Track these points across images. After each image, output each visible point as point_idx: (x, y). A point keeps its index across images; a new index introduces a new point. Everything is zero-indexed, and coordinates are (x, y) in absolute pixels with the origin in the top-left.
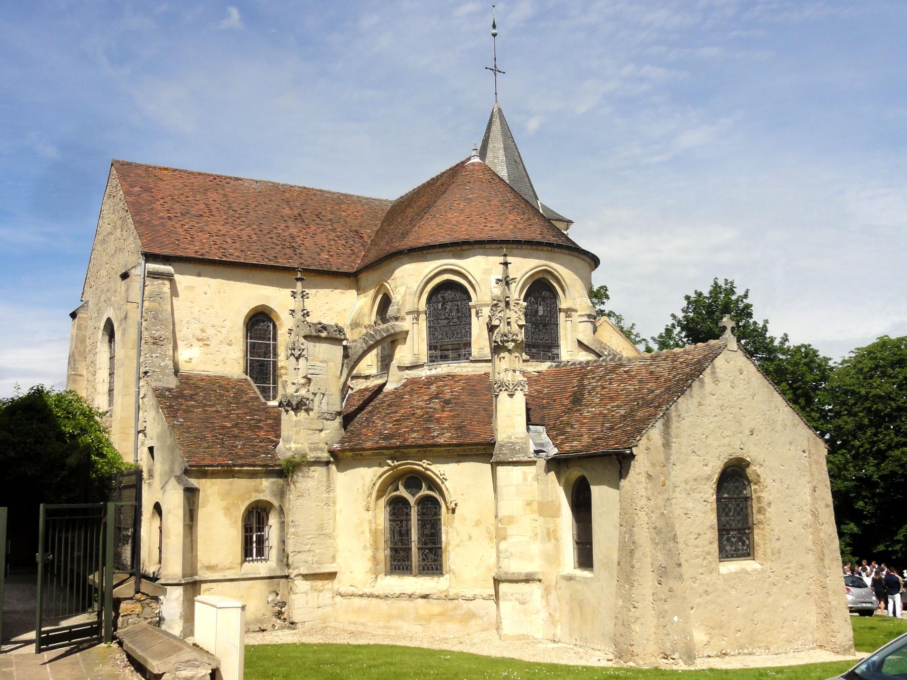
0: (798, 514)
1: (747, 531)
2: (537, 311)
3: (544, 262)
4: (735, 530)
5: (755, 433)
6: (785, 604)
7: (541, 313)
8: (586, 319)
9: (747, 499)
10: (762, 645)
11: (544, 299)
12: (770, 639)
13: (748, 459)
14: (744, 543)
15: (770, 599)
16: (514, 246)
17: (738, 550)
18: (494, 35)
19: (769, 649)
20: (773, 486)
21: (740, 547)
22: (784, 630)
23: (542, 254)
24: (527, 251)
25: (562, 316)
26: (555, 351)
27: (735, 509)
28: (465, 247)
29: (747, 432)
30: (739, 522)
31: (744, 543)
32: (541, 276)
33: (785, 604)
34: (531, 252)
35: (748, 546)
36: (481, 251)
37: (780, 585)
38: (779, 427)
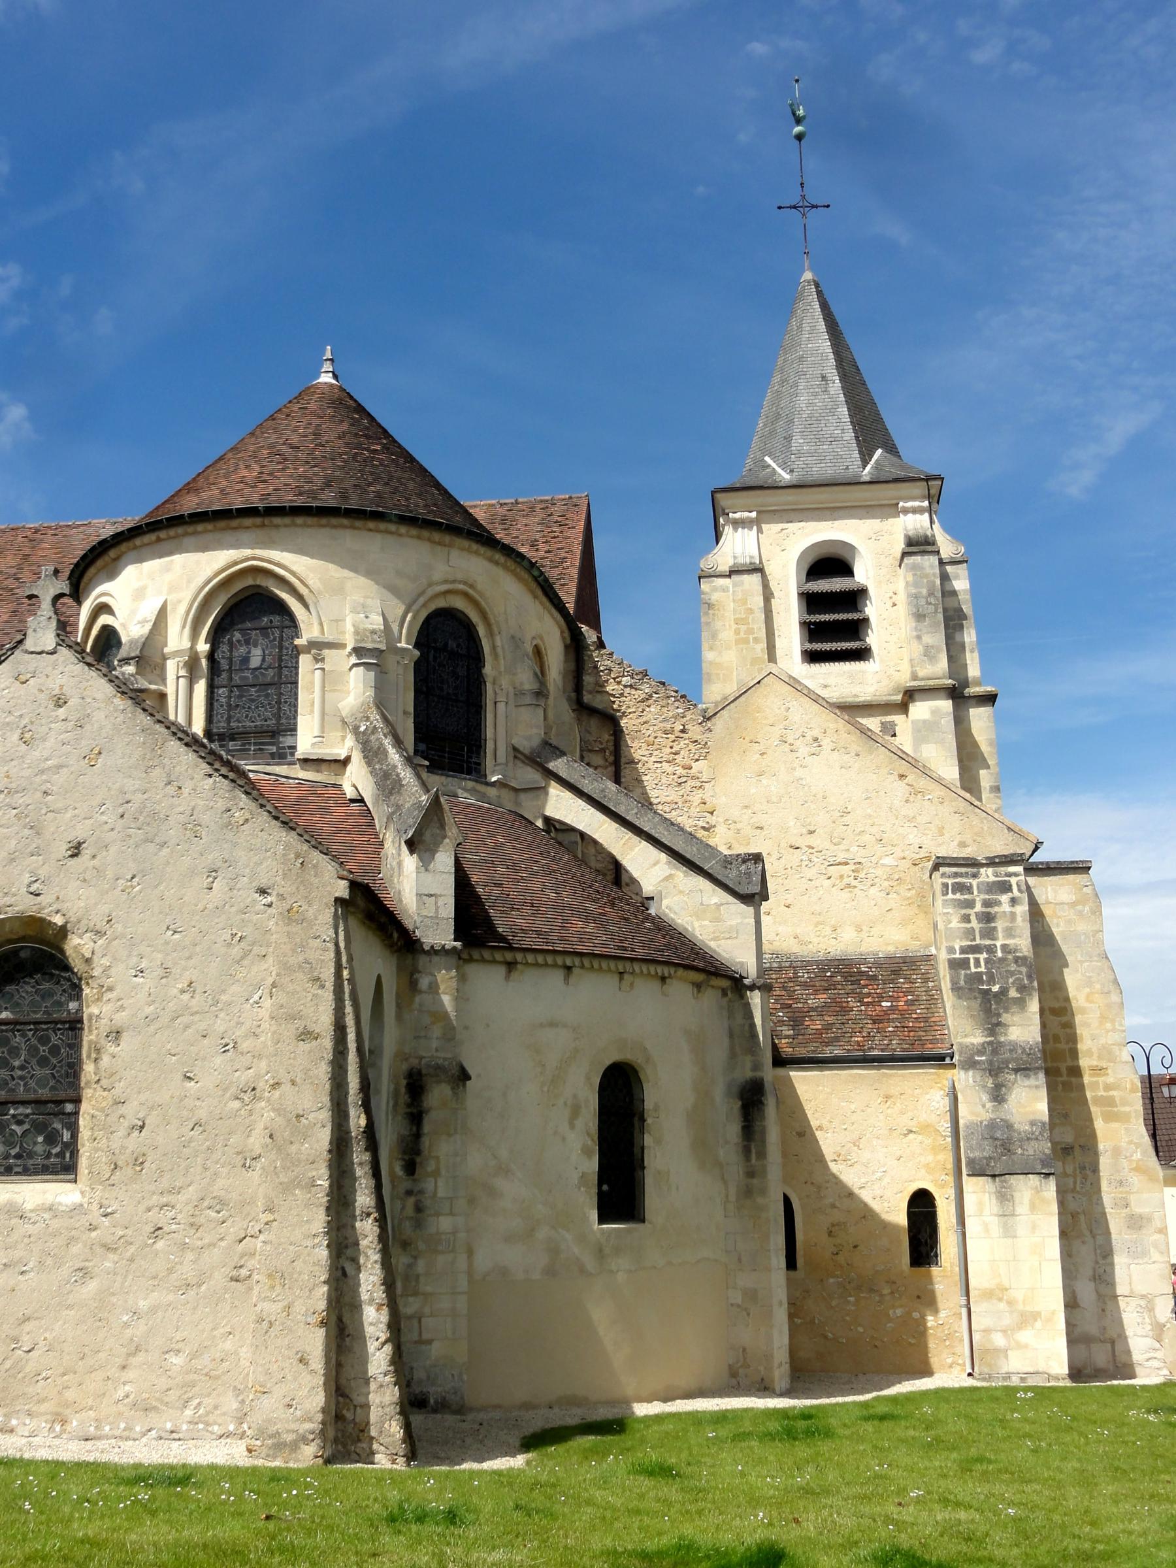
0: (219, 1060)
1: (69, 1107)
2: (246, 660)
3: (248, 552)
4: (23, 1103)
5: (86, 852)
6: (143, 1304)
7: (255, 662)
8: (354, 660)
9: (75, 1025)
10: (43, 1407)
11: (264, 630)
12: (70, 1395)
13: (58, 920)
14: (52, 1139)
15: (92, 1286)
16: (180, 530)
17: (31, 1155)
18: (799, 137)
19: (64, 1422)
20: (135, 987)
21: (39, 1149)
22: (131, 1374)
23: (245, 536)
24: (210, 536)
25: (305, 661)
26: (287, 741)
27: (33, 1051)
28: (112, 553)
29: (62, 849)
30: (41, 1083)
31: (52, 1139)
32: (249, 582)
33: (143, 1304)
34: (218, 535)
35: (66, 1145)
36: (133, 554)
37: (132, 1249)
38: (173, 833)
